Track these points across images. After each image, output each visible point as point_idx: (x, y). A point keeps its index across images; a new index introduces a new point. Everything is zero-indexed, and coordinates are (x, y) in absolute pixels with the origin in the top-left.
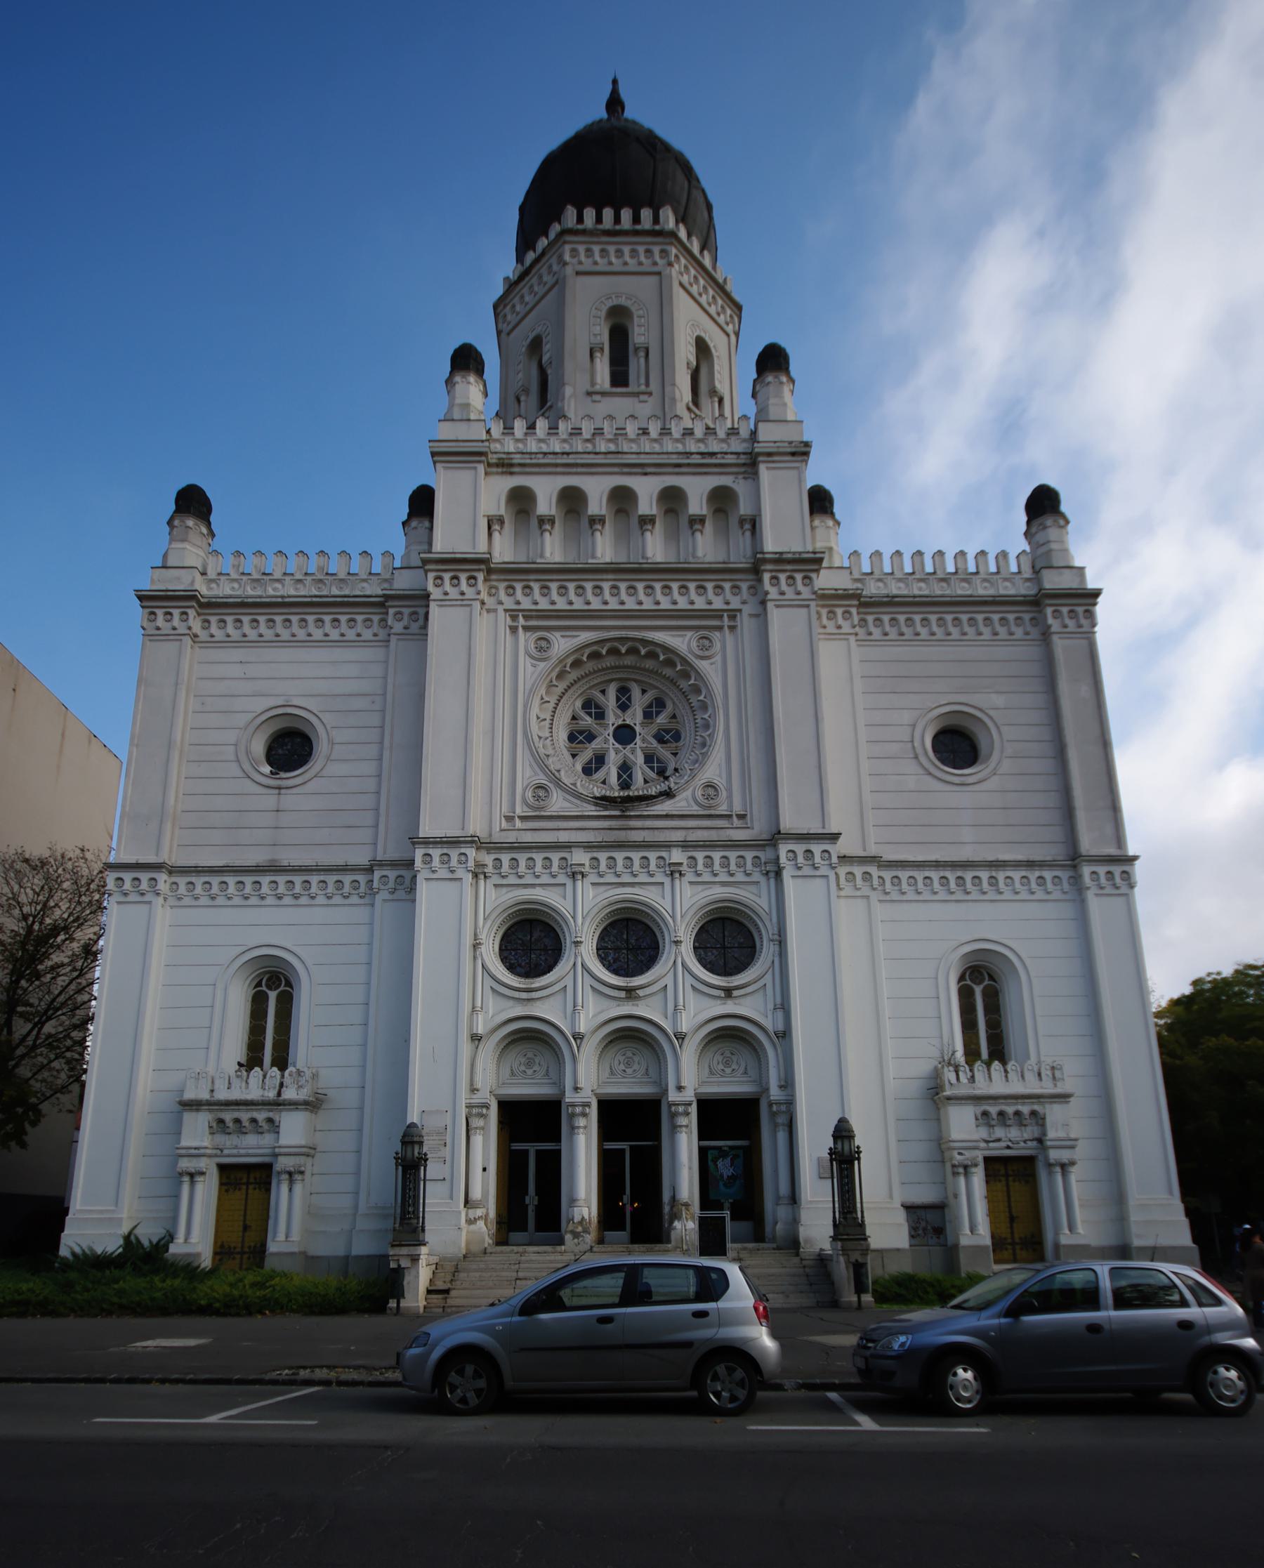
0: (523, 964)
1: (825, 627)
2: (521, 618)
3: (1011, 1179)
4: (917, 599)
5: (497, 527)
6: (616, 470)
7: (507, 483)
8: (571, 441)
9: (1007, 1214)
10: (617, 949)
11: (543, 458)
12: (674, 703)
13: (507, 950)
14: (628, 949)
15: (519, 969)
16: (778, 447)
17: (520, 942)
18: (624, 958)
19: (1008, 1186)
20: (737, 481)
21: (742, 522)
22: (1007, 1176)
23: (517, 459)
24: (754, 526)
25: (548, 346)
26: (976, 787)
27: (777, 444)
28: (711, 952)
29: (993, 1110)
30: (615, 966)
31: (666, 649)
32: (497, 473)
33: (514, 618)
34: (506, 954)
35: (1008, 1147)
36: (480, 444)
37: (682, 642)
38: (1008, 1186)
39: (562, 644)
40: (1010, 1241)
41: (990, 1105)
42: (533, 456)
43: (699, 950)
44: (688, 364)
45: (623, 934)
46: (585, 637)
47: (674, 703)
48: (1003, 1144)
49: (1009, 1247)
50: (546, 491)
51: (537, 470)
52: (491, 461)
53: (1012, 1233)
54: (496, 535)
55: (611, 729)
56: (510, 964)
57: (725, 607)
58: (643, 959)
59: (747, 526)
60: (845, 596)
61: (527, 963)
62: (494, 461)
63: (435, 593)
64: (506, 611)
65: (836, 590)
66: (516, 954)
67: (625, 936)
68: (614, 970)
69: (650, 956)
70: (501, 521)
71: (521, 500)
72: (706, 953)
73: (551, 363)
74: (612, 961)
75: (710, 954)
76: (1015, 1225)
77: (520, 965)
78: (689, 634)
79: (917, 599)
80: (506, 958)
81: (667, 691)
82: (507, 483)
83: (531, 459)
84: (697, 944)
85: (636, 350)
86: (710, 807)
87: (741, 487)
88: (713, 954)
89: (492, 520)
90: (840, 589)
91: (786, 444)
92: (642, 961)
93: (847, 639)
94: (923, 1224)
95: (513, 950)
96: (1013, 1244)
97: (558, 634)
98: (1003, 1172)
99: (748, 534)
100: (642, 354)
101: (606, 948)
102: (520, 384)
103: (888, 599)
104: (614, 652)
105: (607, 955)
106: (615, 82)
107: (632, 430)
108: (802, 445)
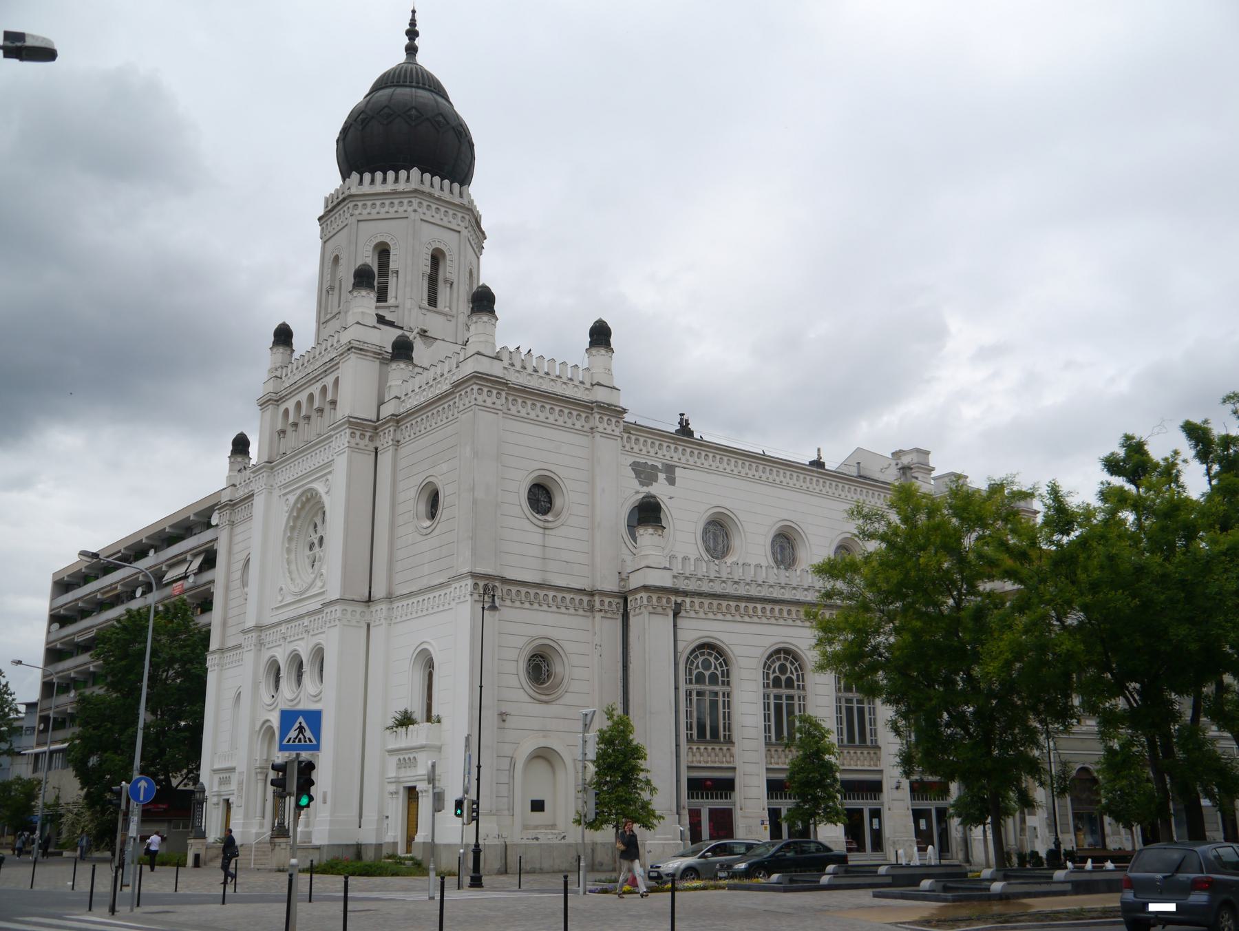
5: (281, 435)
39: (292, 498)
46: (299, 492)
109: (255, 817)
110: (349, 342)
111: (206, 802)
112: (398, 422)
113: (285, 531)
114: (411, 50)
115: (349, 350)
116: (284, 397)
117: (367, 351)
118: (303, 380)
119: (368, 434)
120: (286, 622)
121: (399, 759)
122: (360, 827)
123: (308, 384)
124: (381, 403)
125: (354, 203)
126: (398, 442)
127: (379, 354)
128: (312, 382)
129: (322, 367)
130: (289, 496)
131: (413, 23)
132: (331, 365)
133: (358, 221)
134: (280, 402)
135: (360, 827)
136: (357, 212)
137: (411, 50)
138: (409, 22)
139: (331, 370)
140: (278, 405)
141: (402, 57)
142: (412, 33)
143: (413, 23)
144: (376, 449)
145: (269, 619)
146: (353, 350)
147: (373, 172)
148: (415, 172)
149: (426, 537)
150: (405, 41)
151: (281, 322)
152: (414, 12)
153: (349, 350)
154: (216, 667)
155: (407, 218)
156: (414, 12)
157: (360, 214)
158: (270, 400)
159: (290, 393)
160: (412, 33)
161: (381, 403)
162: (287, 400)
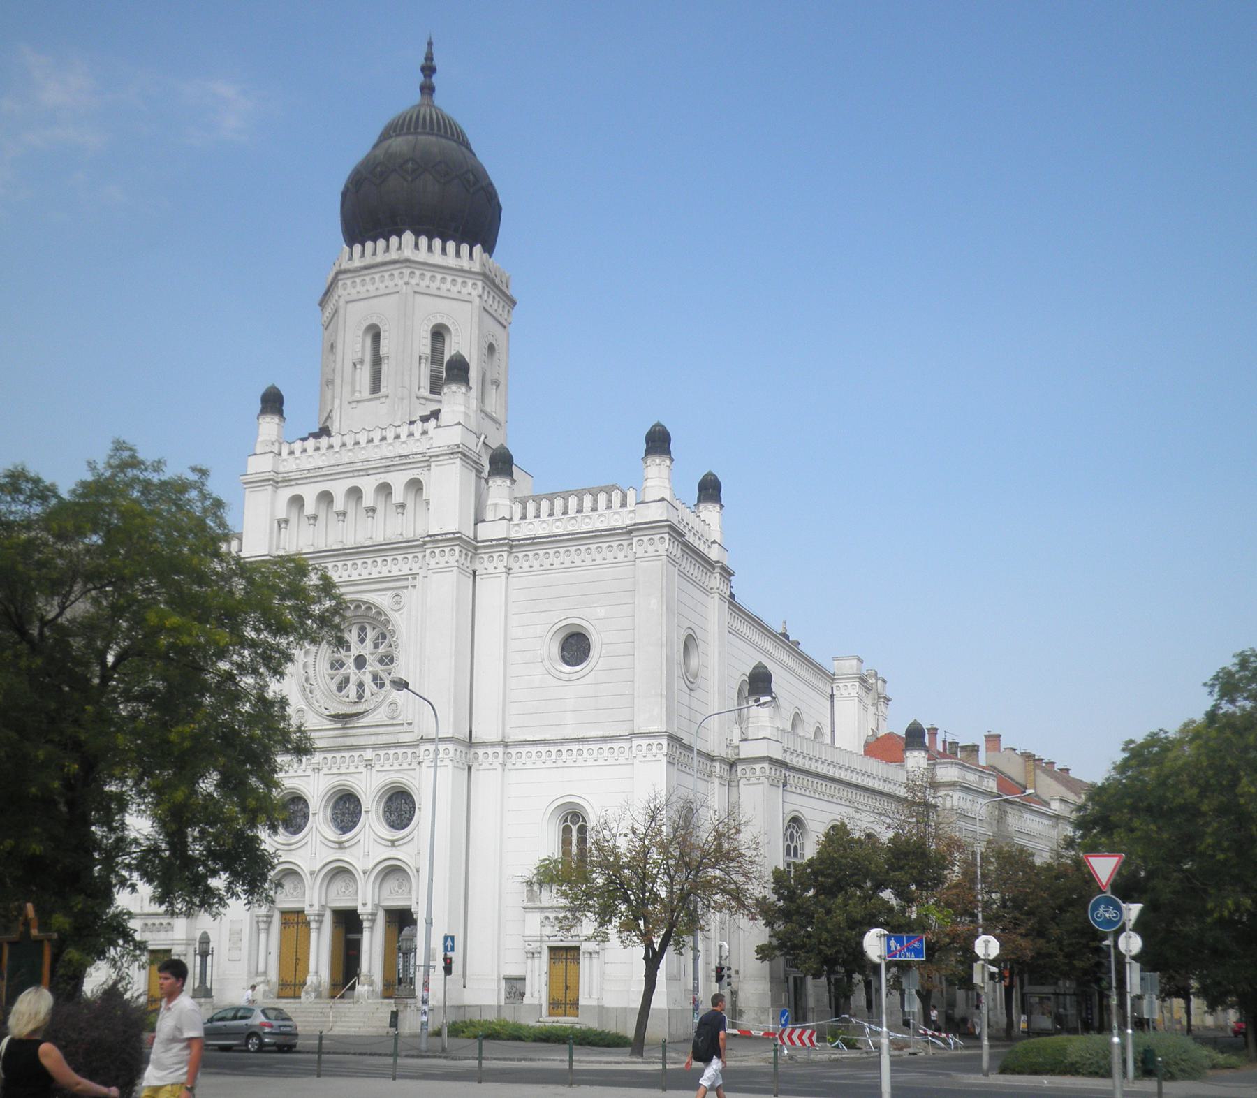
3: (569, 961)
5: (283, 526)
7: (286, 493)
19: (566, 965)
35: (562, 940)
36: (267, 474)
37: (382, 600)
38: (566, 965)
41: (550, 912)
48: (559, 939)
50: (309, 493)
51: (305, 481)
57: (410, 572)
70: (286, 521)
71: (297, 501)
76: (568, 991)
78: (389, 592)
82: (286, 493)
86: (393, 718)
94: (515, 990)
96: (565, 1004)
98: (564, 956)
105: (337, 817)
110: (458, 446)
111: (212, 954)
112: (512, 547)
114: (428, 89)
116: (291, 480)
117: (469, 458)
119: (470, 554)
122: (464, 987)
123: (351, 474)
124: (479, 520)
125: (412, 270)
126: (509, 569)
127: (476, 463)
128: (361, 473)
131: (429, 58)
132: (401, 462)
134: (280, 485)
135: (464, 987)
136: (413, 282)
137: (428, 89)
138: (424, 55)
140: (277, 488)
141: (414, 97)
142: (429, 69)
143: (429, 58)
144: (474, 572)
146: (460, 455)
147: (417, 234)
148: (478, 249)
150: (420, 78)
151: (269, 384)
152: (430, 44)
155: (471, 302)
156: (430, 44)
157: (418, 285)
158: (269, 480)
159: (306, 478)
160: (429, 69)
161: (479, 520)
162: (297, 484)
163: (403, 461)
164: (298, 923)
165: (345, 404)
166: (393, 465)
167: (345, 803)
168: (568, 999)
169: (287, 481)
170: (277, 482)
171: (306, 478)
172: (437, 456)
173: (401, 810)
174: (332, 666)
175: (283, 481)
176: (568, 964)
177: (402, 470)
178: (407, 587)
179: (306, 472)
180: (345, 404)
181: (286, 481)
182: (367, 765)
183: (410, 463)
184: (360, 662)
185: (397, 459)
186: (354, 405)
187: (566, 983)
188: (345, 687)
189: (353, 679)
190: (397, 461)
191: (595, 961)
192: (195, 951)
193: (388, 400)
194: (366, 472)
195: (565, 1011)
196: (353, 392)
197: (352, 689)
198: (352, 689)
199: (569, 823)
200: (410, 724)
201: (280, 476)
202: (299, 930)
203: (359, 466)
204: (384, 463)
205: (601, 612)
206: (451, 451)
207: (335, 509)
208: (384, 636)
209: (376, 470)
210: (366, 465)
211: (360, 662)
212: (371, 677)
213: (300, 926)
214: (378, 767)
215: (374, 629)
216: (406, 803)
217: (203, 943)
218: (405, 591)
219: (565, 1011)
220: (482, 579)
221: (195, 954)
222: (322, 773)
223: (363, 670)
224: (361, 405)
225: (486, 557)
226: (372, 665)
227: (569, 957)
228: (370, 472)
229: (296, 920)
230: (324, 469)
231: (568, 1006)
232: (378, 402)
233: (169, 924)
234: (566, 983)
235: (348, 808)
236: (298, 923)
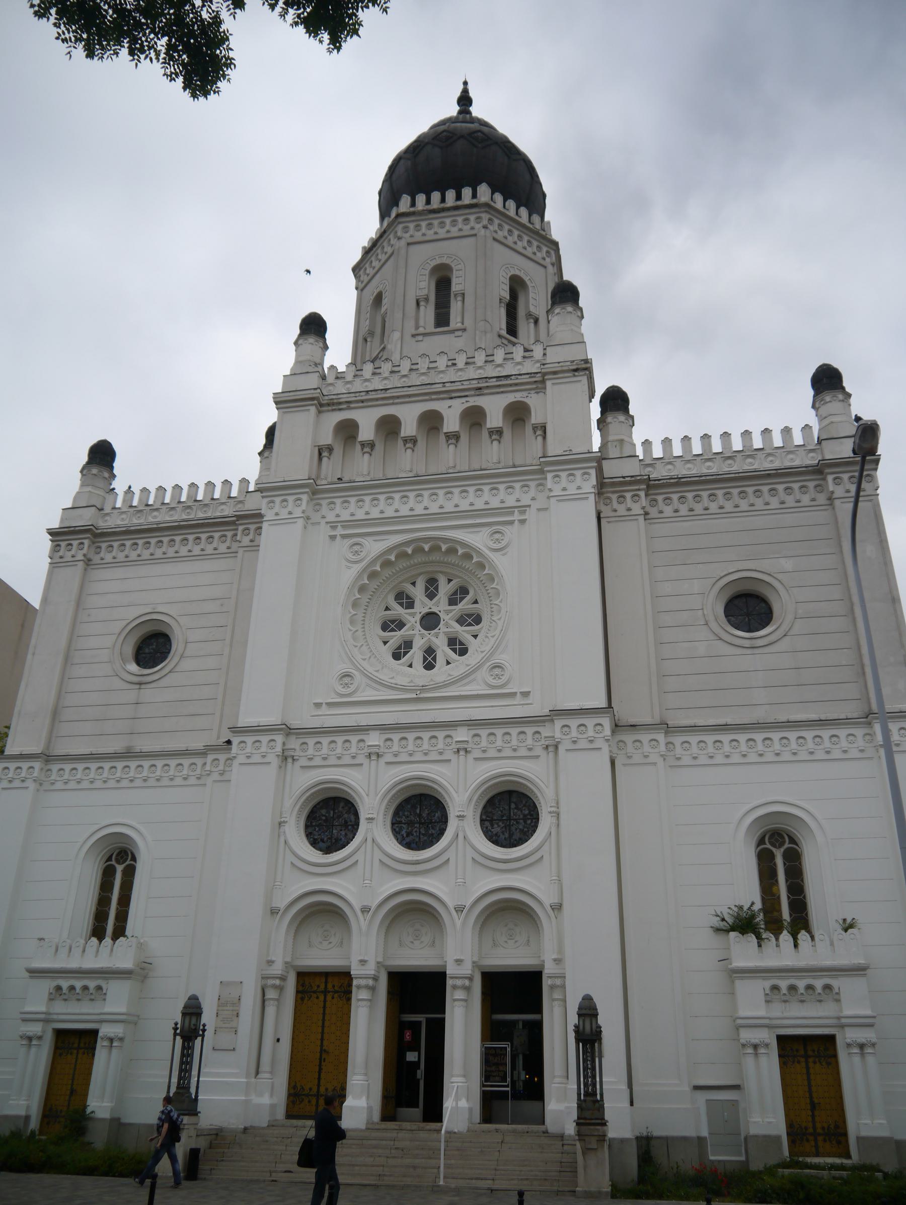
0: (325, 839)
1: (615, 511)
2: (339, 527)
3: (811, 1060)
4: (703, 478)
5: (325, 454)
6: (427, 397)
7: (335, 418)
8: (391, 378)
9: (808, 1101)
10: (410, 823)
11: (366, 395)
12: (475, 590)
13: (312, 826)
14: (420, 823)
15: (321, 844)
16: (562, 366)
17: (324, 818)
18: (416, 831)
19: (808, 1068)
20: (529, 395)
21: (535, 428)
22: (807, 1057)
23: (344, 398)
24: (545, 432)
25: (386, 299)
26: (766, 650)
27: (561, 364)
28: (497, 824)
29: (784, 984)
30: (408, 840)
31: (464, 544)
32: (328, 411)
33: (334, 528)
34: (310, 830)
36: (313, 391)
38: (808, 1068)
39: (374, 547)
40: (811, 1130)
42: (357, 395)
43: (486, 822)
44: (500, 299)
45: (416, 808)
47: (475, 590)
49: (811, 1138)
52: (323, 402)
53: (814, 1122)
54: (325, 460)
55: (418, 617)
56: (315, 839)
58: (434, 832)
59: (539, 432)
60: (633, 481)
61: (329, 838)
62: (325, 402)
63: (269, 515)
64: (327, 523)
65: (624, 477)
66: (319, 830)
67: (418, 811)
68: (406, 844)
69: (440, 830)
70: (330, 449)
71: (347, 430)
72: (492, 825)
73: (386, 313)
74: (405, 835)
75: (496, 826)
76: (816, 1113)
77: (322, 841)
79: (703, 478)
80: (311, 833)
81: (468, 580)
82: (335, 418)
83: (356, 397)
84: (484, 817)
85: (455, 295)
87: (533, 400)
88: (499, 826)
89: (322, 449)
90: (627, 477)
91: (569, 363)
92: (432, 834)
93: (637, 520)
95: (318, 826)
97: (370, 539)
98: (802, 1052)
99: (540, 439)
100: (459, 298)
101: (400, 822)
102: (367, 328)
103: (676, 480)
104: (419, 550)
105: (401, 829)
106: (465, 83)
107: (442, 362)
108: (583, 362)
109: (554, 1077)
111: (203, 1036)
113: (350, 589)
115: (576, 370)
116: (340, 403)
118: (424, 387)
120: (380, 729)
121: (775, 988)
128: (442, 396)
129: (494, 380)
130: (367, 542)
131: (465, 92)
133: (409, 244)
139: (502, 390)
143: (465, 92)
145: (303, 718)
149: (749, 651)
153: (576, 370)
154: (30, 784)
156: (465, 83)
158: (312, 399)
159: (362, 401)
163: (503, 383)
164: (325, 992)
165: (407, 337)
166: (487, 387)
167: (414, 807)
168: (818, 1125)
169: (334, 405)
170: (321, 405)
171: (362, 401)
172: (555, 373)
173: (509, 819)
174: (385, 627)
175: (328, 405)
176: (811, 1065)
177: (498, 393)
178: (511, 523)
179: (363, 394)
180: (407, 337)
181: (333, 404)
182: (458, 751)
183: (511, 385)
184: (430, 621)
185: (494, 380)
186: (420, 338)
187: (811, 1097)
188: (405, 653)
189: (419, 645)
190: (493, 382)
191: (870, 1060)
192: (175, 1029)
193: (465, 334)
194: (450, 395)
195: (816, 1146)
196: (417, 328)
197: (416, 654)
198: (416, 654)
199: (768, 846)
200: (526, 694)
201: (326, 398)
202: (328, 1004)
203: (439, 388)
204: (475, 384)
205: (788, 564)
206: (574, 367)
207: (403, 434)
208: (463, 591)
209: (460, 394)
210: (449, 387)
211: (430, 621)
212: (446, 642)
213: (329, 997)
214: (477, 754)
215: (450, 581)
216: (517, 808)
217: (191, 1014)
218: (509, 527)
219: (816, 1146)
220: (609, 522)
221: (175, 1035)
222: (382, 761)
223: (436, 630)
224: (427, 339)
225: (614, 497)
226: (449, 624)
227: (810, 1053)
228: (454, 395)
229: (322, 987)
230: (388, 392)
231: (820, 1138)
232: (452, 335)
233: (99, 988)
234: (811, 1097)
235: (420, 815)
236: (325, 992)
